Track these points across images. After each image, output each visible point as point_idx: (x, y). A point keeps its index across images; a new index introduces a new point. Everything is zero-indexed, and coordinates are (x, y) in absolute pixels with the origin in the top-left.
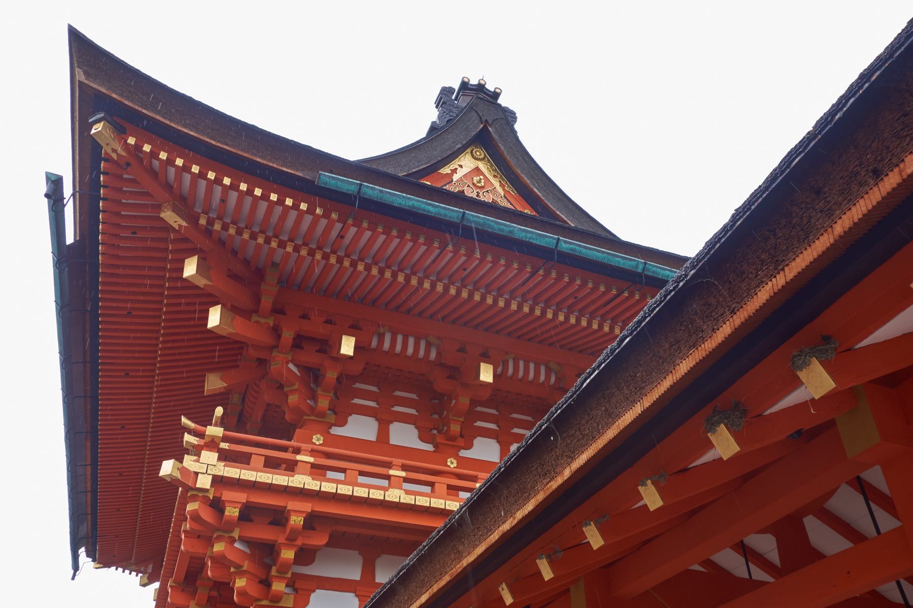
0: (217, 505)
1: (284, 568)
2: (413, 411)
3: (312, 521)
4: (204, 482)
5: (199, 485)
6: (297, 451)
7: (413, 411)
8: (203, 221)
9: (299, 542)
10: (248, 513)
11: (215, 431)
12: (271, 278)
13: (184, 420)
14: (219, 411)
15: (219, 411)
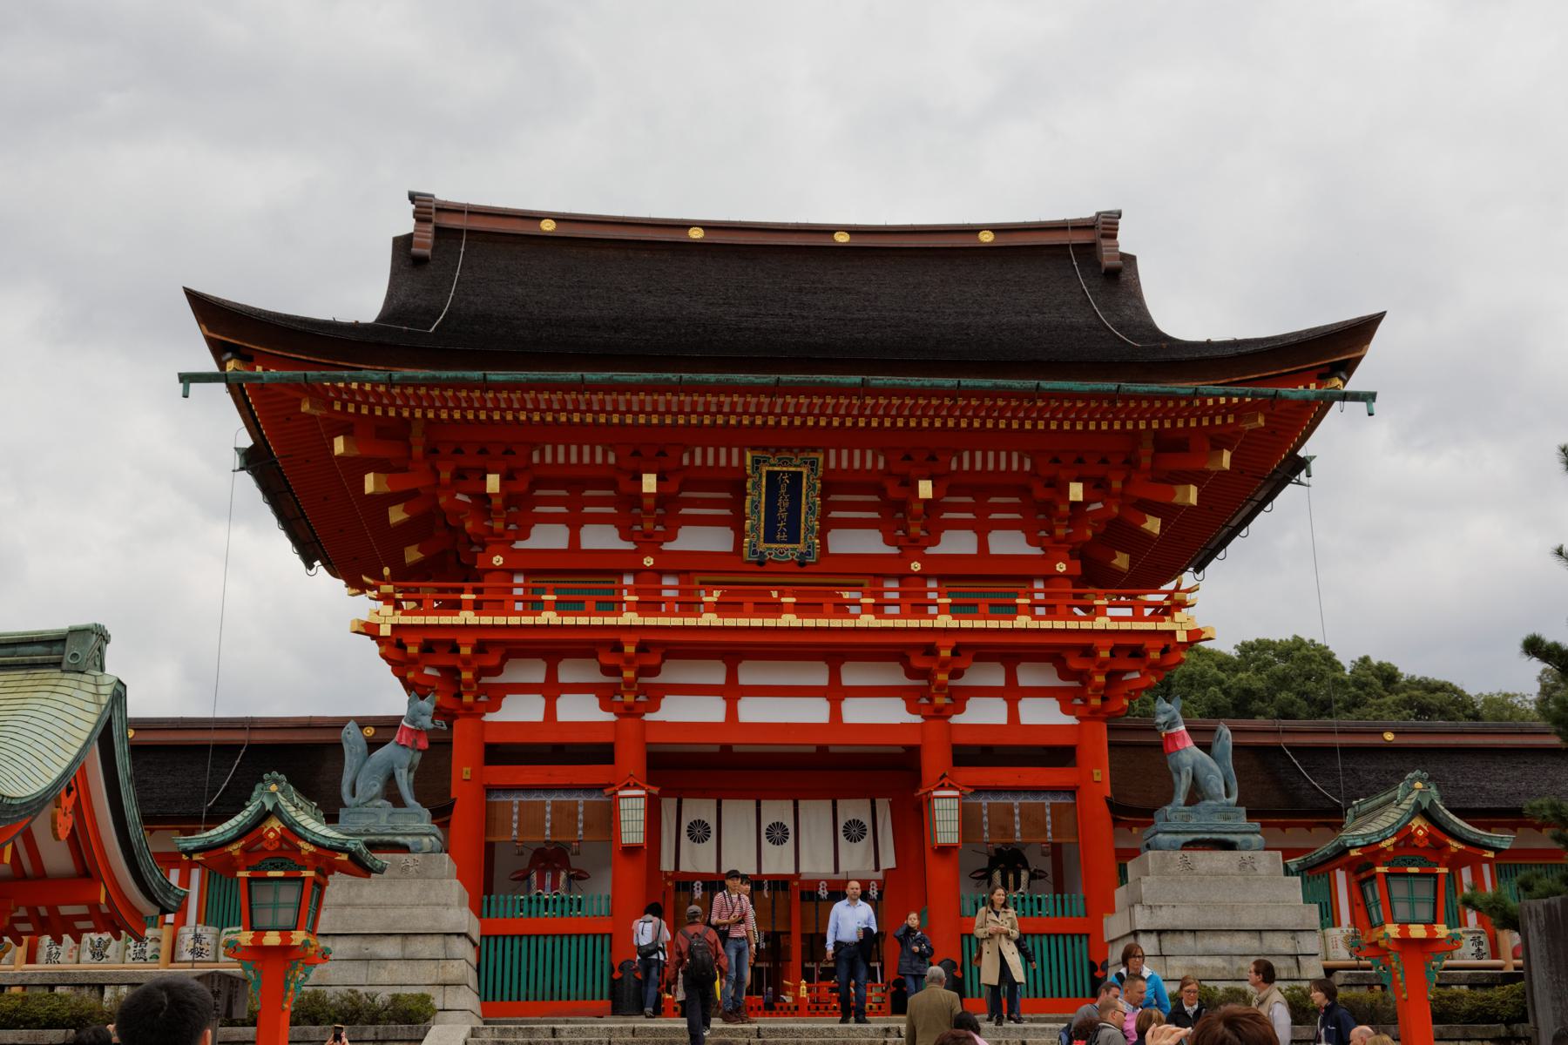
0: (401, 646)
1: (468, 685)
2: (611, 510)
3: (481, 648)
4: (385, 631)
5: (382, 633)
6: (462, 591)
7: (611, 510)
8: (337, 407)
9: (476, 665)
10: (428, 648)
11: (387, 588)
12: (417, 432)
13: (365, 579)
14: (386, 571)
15: (386, 571)
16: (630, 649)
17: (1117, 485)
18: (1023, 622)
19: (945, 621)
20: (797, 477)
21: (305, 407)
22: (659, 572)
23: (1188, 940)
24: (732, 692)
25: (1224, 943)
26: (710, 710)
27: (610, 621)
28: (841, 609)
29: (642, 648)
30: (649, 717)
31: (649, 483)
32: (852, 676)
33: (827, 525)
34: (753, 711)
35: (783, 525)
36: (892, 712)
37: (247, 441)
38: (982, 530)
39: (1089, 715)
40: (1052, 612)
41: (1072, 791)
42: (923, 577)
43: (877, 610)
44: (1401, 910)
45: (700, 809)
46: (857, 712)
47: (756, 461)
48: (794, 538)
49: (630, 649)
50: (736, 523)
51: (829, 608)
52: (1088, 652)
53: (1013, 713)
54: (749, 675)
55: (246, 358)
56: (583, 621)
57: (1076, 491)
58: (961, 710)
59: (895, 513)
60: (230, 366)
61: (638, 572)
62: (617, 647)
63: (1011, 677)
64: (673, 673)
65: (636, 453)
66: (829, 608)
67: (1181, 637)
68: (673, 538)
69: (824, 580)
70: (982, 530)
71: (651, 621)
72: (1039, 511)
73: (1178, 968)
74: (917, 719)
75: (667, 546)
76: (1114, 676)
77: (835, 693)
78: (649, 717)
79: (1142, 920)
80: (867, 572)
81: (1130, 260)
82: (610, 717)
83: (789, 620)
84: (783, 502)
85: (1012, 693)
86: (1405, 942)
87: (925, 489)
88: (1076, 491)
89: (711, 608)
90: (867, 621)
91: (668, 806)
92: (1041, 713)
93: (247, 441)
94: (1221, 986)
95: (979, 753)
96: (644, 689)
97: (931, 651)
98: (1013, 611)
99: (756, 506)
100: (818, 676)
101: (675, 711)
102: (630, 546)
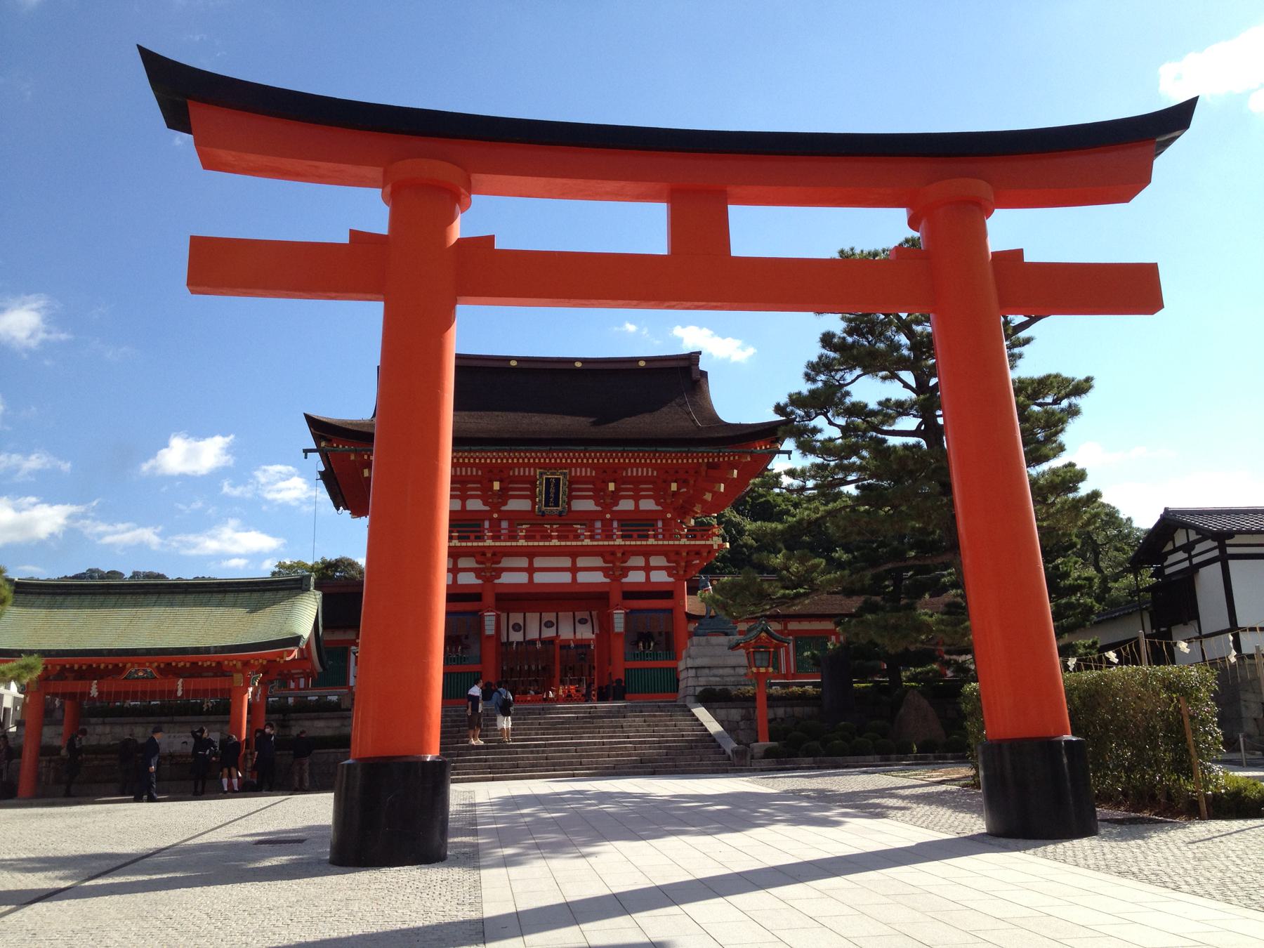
16: (489, 555)
17: (692, 482)
18: (651, 541)
19: (619, 542)
20: (558, 480)
21: (352, 457)
22: (499, 520)
23: (707, 671)
24: (531, 570)
25: (721, 672)
26: (522, 578)
27: (481, 544)
28: (577, 537)
29: (494, 554)
30: (497, 581)
31: (496, 486)
32: (581, 562)
33: (571, 498)
34: (540, 578)
35: (552, 499)
36: (598, 577)
37: (323, 469)
38: (637, 499)
39: (679, 579)
40: (664, 539)
41: (671, 611)
42: (611, 520)
43: (592, 538)
44: (758, 663)
45: (516, 618)
46: (583, 577)
47: (541, 474)
48: (557, 504)
49: (489, 555)
50: (532, 497)
51: (571, 537)
52: (678, 553)
53: (648, 577)
54: (539, 562)
55: (329, 441)
56: (469, 544)
57: (674, 487)
58: (626, 576)
59: (599, 494)
60: (323, 444)
61: (491, 520)
62: (484, 554)
63: (647, 562)
64: (506, 562)
65: (490, 471)
66: (571, 537)
67: (715, 547)
68: (505, 504)
69: (568, 523)
70: (637, 499)
71: (498, 544)
72: (660, 493)
73: (702, 681)
74: (608, 580)
75: (504, 508)
76: (688, 565)
77: (574, 570)
78: (497, 581)
79: (690, 663)
80: (587, 519)
81: (704, 374)
82: (480, 582)
83: (555, 542)
84: (552, 490)
85: (648, 569)
86: (758, 673)
87: (612, 486)
88: (674, 487)
89: (522, 538)
90: (587, 542)
91: (504, 616)
92: (660, 577)
93: (323, 469)
94: (718, 688)
95: (633, 594)
96: (494, 570)
97: (613, 554)
98: (647, 537)
99: (540, 492)
100: (566, 562)
101: (507, 578)
102: (487, 508)
